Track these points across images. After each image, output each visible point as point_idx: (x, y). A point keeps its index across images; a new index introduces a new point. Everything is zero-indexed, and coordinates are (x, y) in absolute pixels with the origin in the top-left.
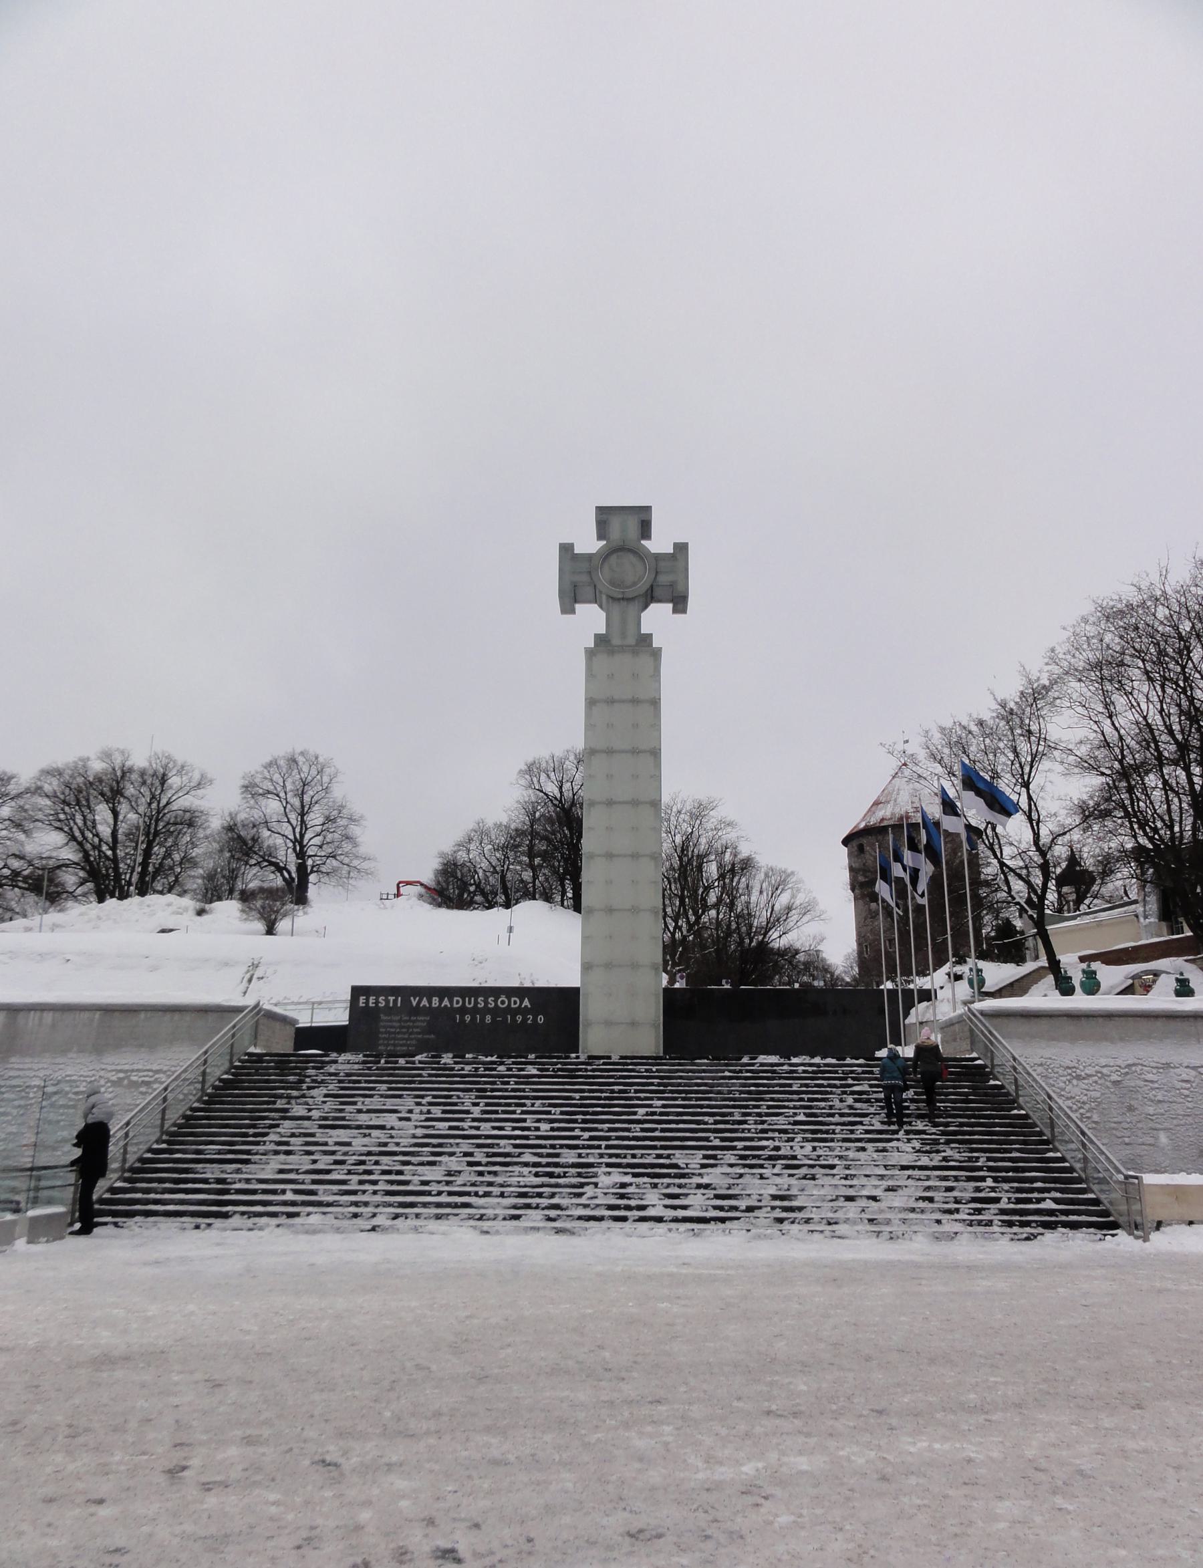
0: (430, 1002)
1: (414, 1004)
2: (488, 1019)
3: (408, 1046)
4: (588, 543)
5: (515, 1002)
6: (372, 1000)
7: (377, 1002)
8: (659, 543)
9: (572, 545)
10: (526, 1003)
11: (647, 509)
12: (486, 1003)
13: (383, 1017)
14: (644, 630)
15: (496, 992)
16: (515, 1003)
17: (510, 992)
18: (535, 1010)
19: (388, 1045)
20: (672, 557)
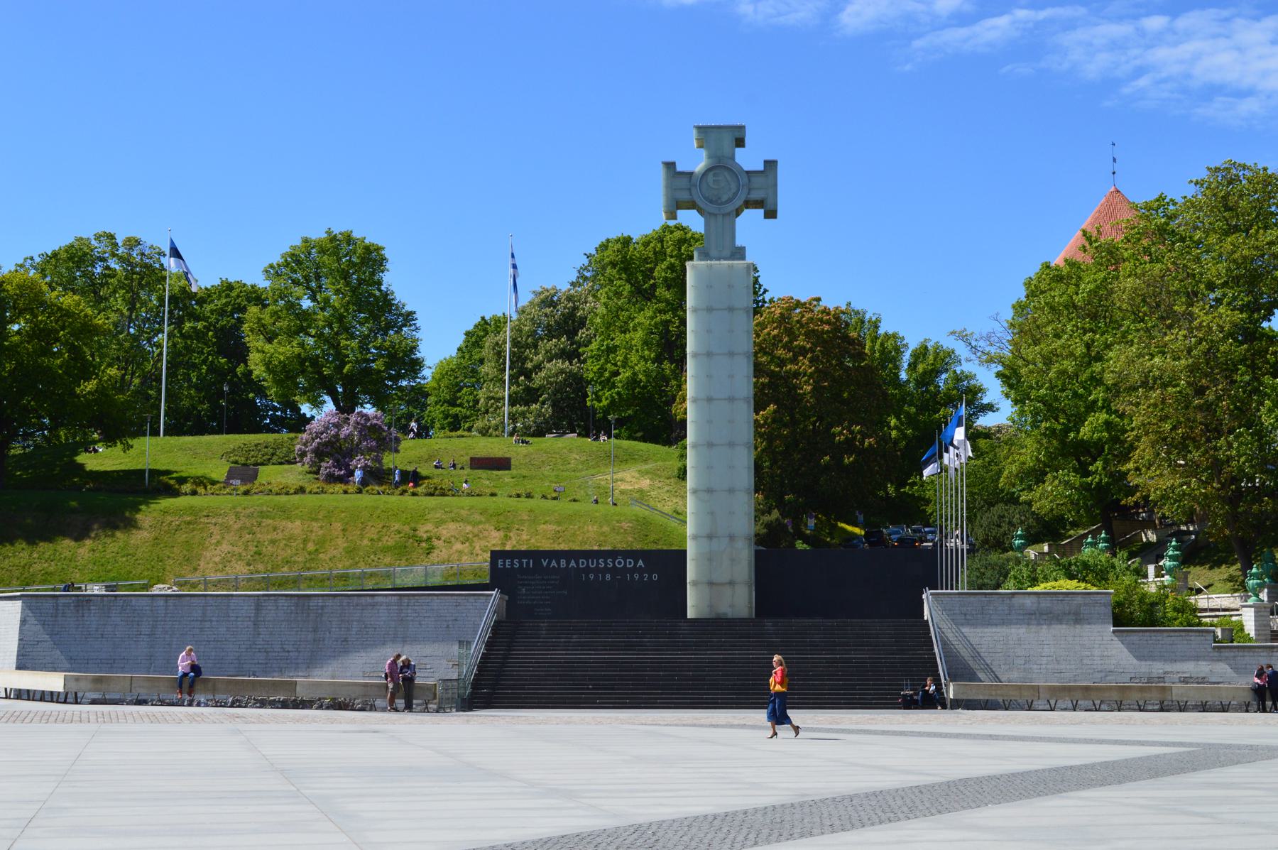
0: (558, 563)
2: (608, 577)
5: (630, 563)
7: (512, 564)
10: (641, 563)
11: (742, 128)
12: (606, 563)
14: (739, 243)
15: (613, 554)
17: (627, 554)
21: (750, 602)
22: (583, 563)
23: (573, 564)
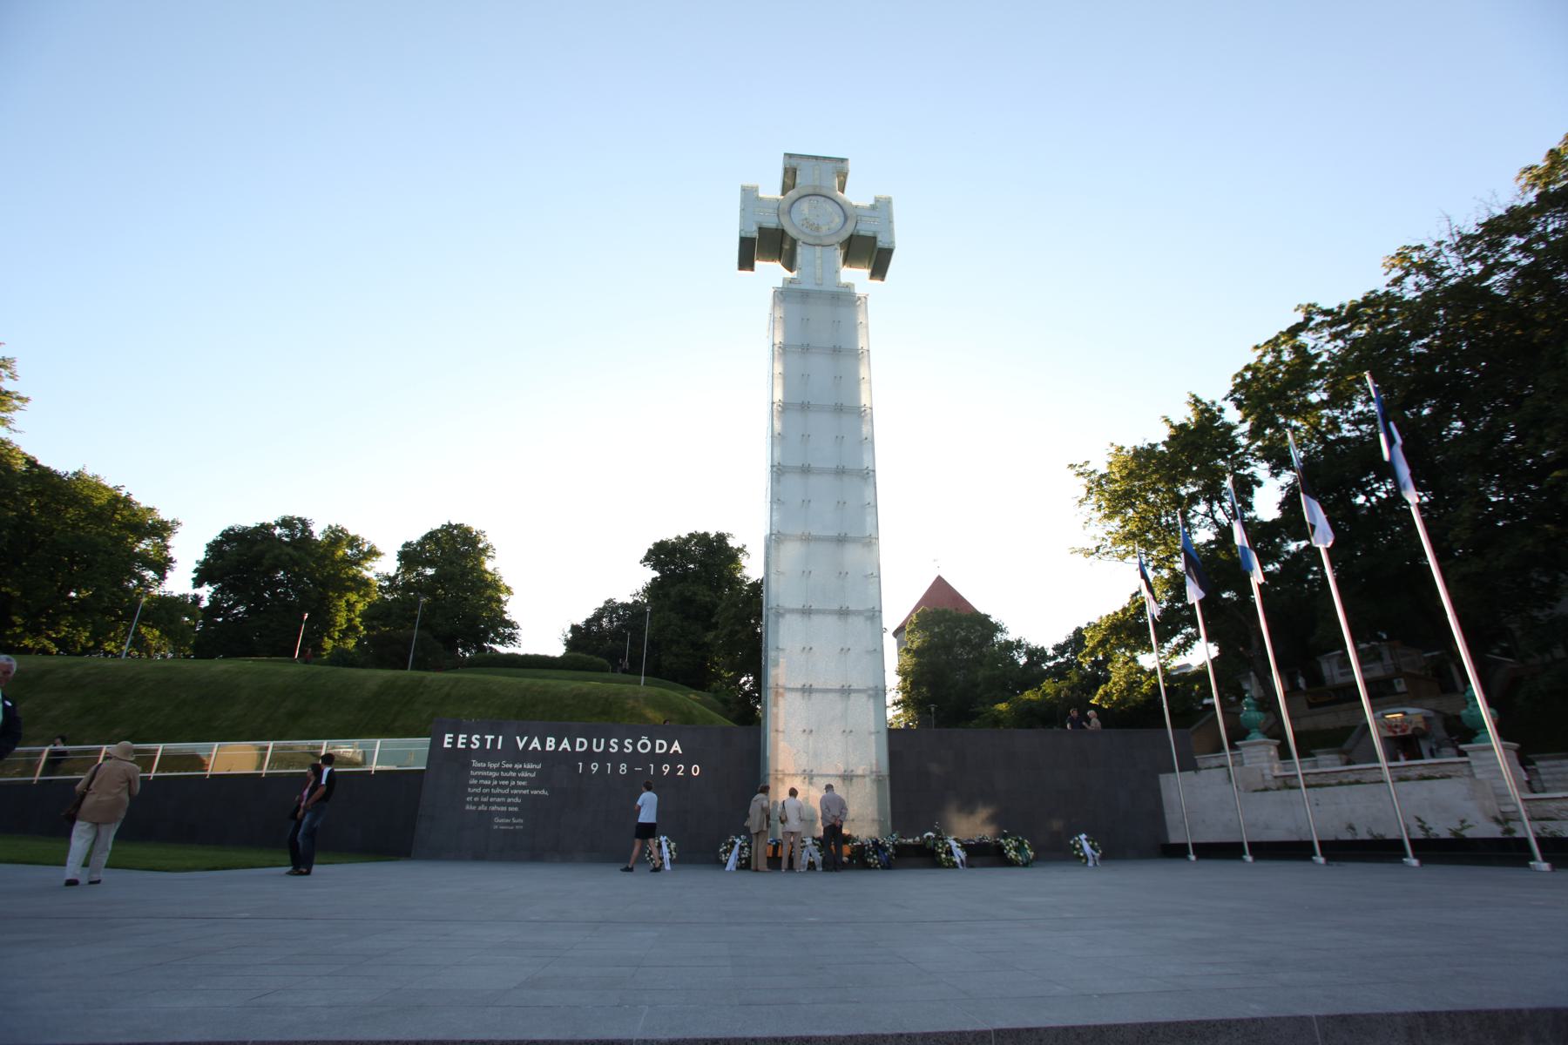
0: (543, 744)
1: (521, 746)
2: (623, 768)
3: (509, 805)
4: (771, 188)
6: (462, 738)
7: (469, 742)
8: (858, 194)
9: (754, 190)
10: (676, 747)
11: (843, 160)
12: (621, 746)
13: (475, 764)
16: (661, 746)
18: (687, 758)
19: (479, 803)
20: (873, 207)
21: (880, 811)
22: (581, 745)
23: (565, 744)
